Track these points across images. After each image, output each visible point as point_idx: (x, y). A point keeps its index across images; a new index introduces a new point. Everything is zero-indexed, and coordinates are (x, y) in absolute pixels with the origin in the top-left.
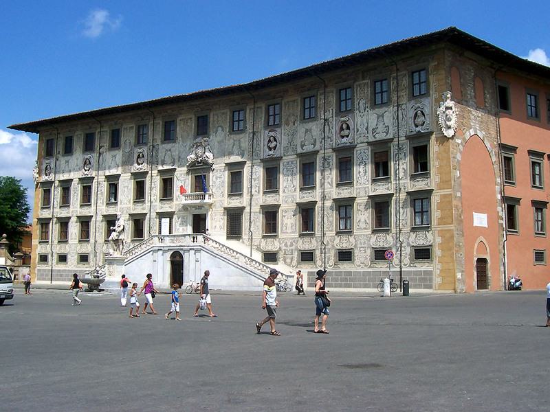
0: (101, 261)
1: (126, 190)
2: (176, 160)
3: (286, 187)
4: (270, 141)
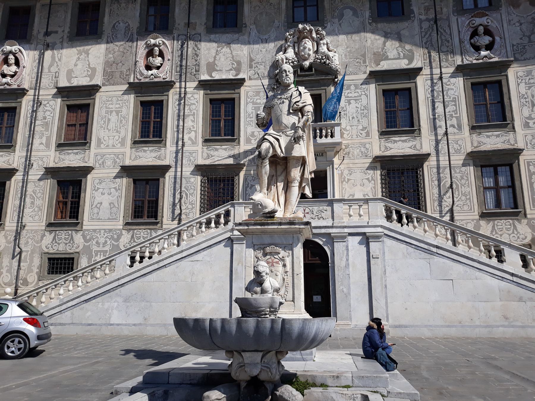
0: (36, 270)
1: (114, 118)
2: (245, 67)
3: (530, 118)
4: (475, 33)
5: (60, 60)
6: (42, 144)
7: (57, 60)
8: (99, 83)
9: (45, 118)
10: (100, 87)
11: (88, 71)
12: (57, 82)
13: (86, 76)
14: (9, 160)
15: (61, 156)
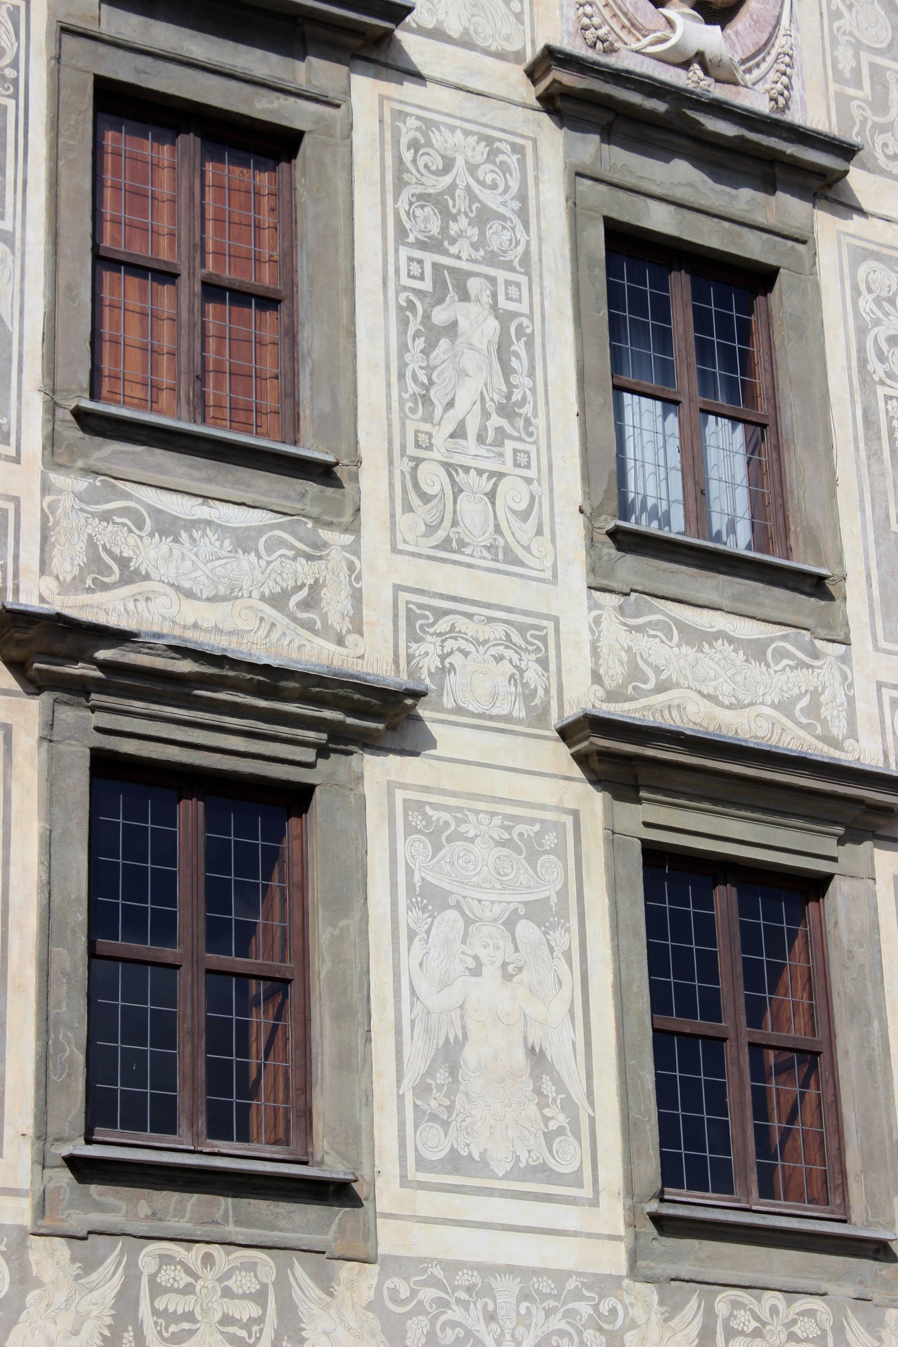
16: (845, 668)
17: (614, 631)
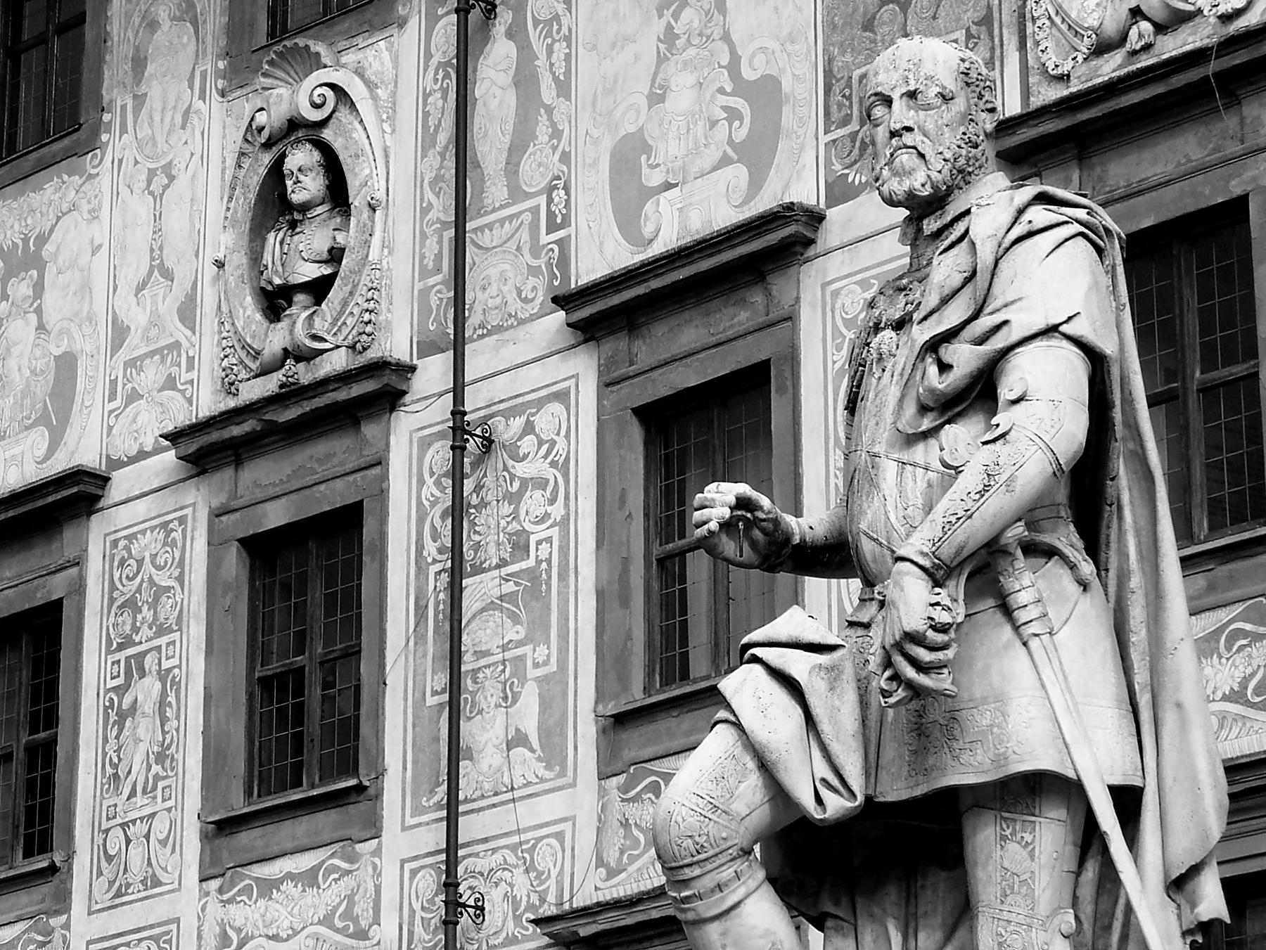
5: (564, 88)
6: (518, 740)
7: (548, 93)
8: (807, 192)
9: (520, 546)
10: (816, 218)
11: (733, 115)
12: (564, 261)
13: (725, 161)
14: (350, 898)
15: (633, 811)
16: (377, 860)
17: (215, 909)
